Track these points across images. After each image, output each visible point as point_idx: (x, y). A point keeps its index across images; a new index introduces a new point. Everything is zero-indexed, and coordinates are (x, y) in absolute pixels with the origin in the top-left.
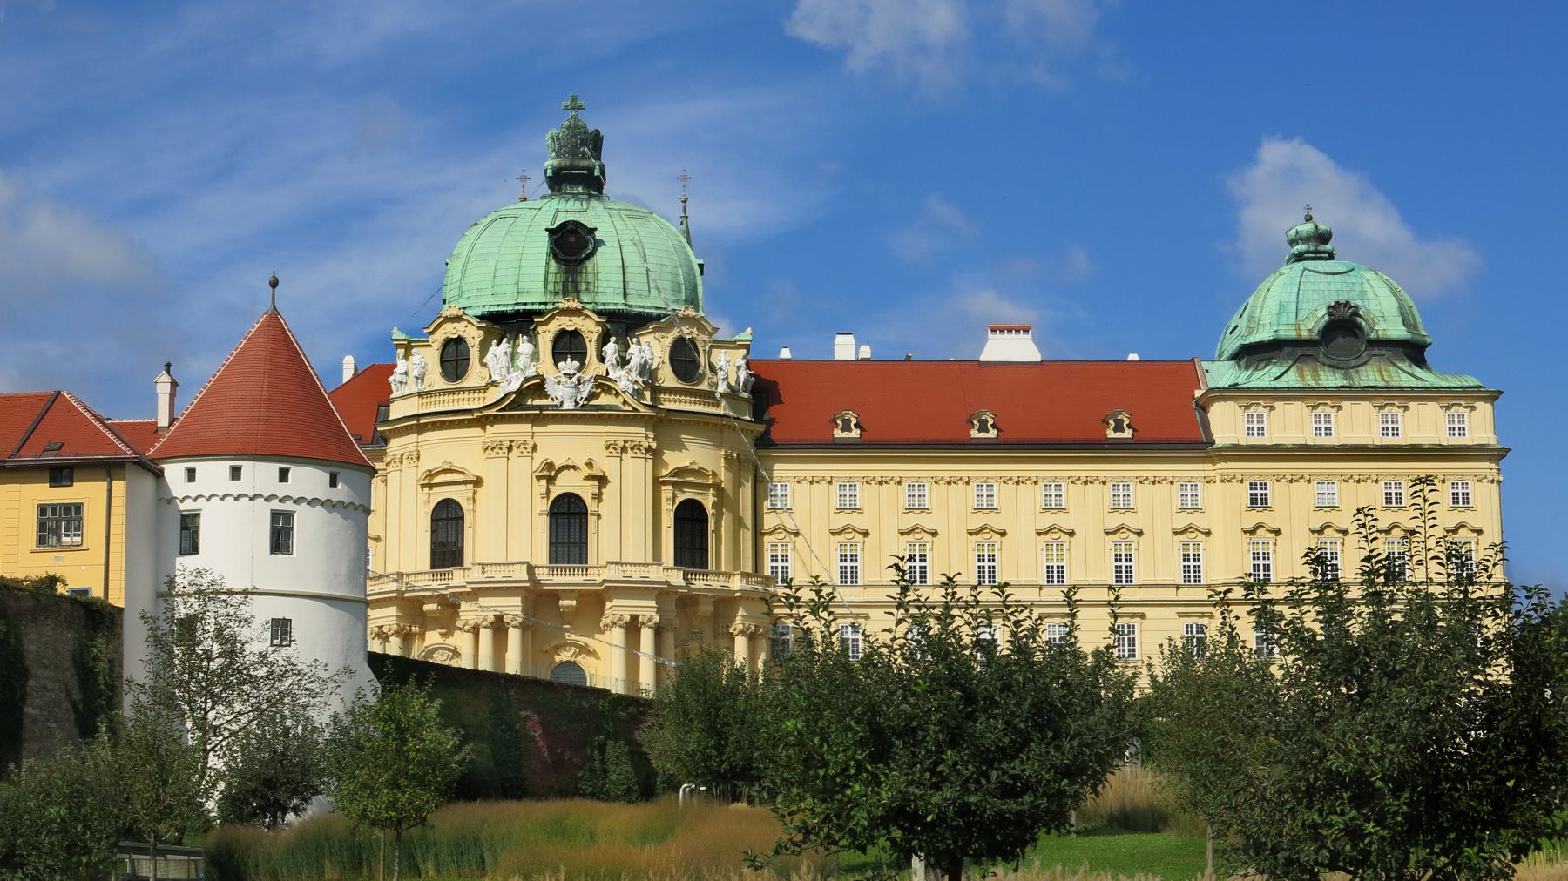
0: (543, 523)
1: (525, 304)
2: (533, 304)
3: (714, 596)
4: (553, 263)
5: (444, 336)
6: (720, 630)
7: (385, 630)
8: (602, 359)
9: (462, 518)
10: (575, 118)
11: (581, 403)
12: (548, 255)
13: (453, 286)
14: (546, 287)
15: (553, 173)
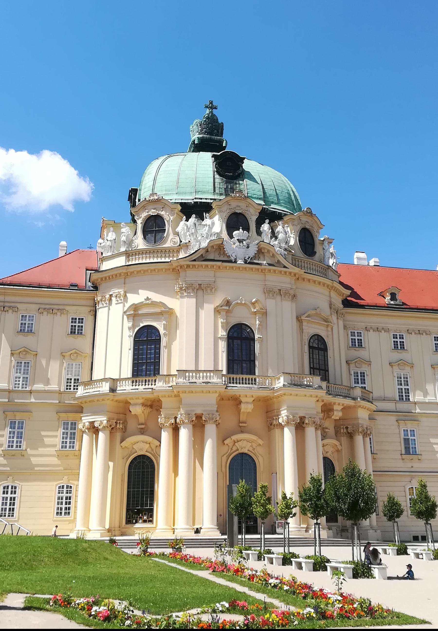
0: (222, 346)
1: (201, 199)
2: (206, 199)
3: (343, 405)
4: (217, 176)
5: (147, 214)
6: (342, 430)
7: (96, 425)
8: (259, 233)
9: (158, 341)
10: (212, 112)
11: (249, 261)
12: (214, 172)
13: (146, 190)
14: (214, 190)
15: (199, 141)
